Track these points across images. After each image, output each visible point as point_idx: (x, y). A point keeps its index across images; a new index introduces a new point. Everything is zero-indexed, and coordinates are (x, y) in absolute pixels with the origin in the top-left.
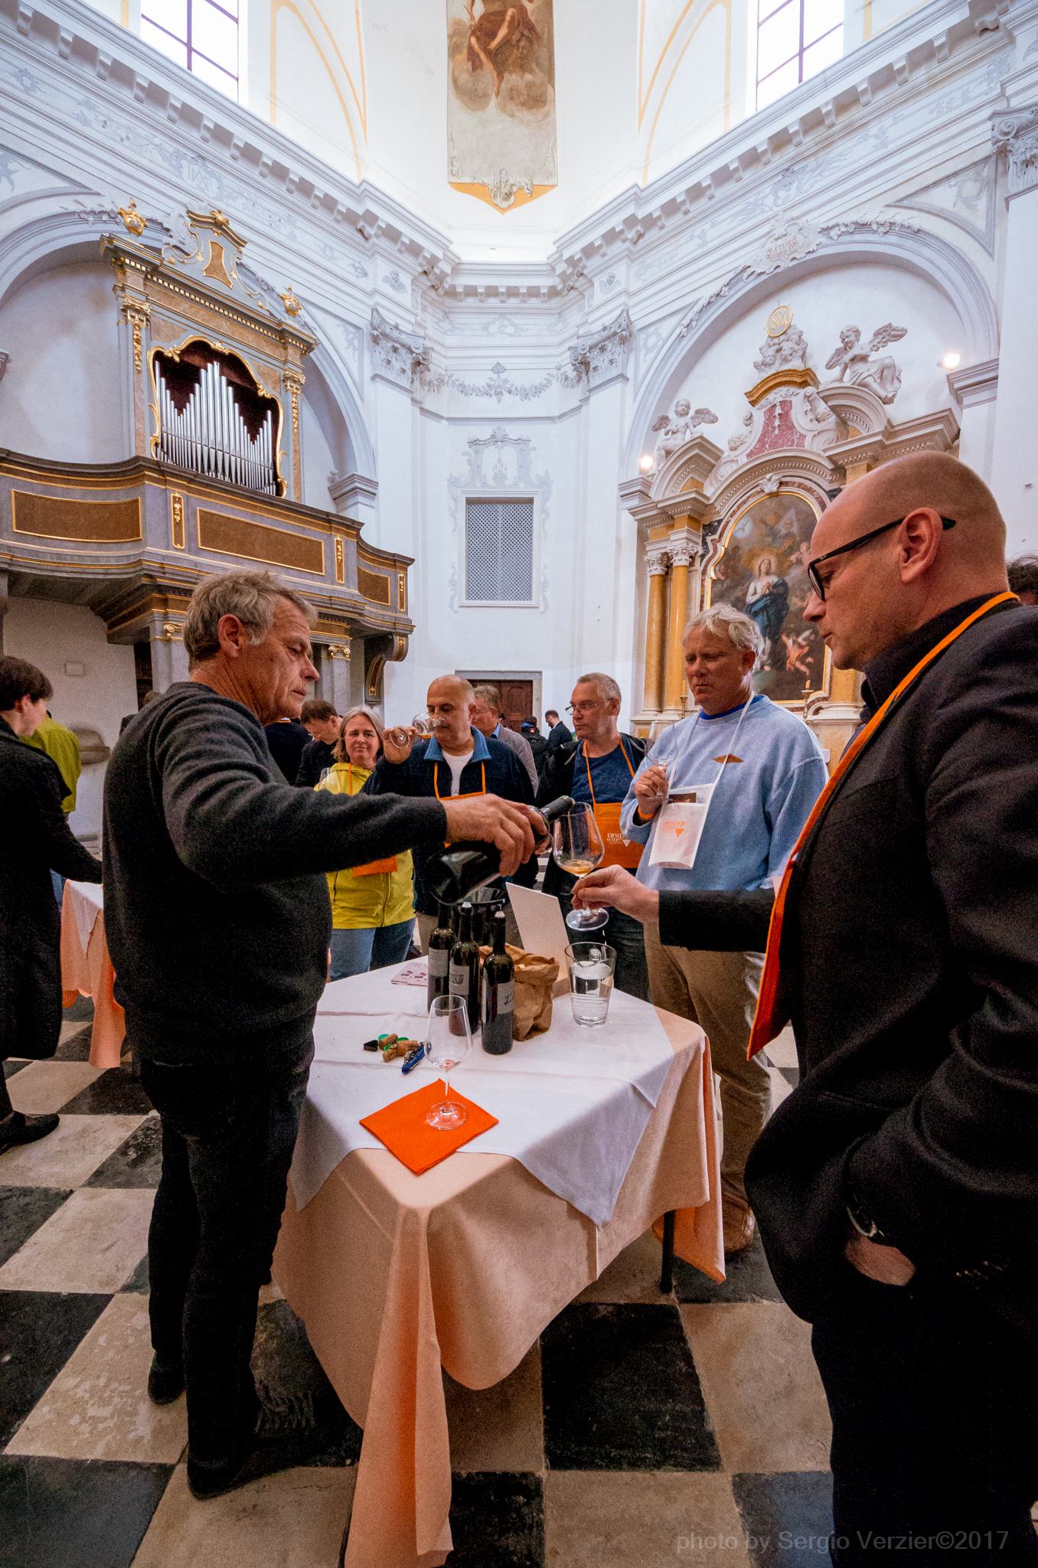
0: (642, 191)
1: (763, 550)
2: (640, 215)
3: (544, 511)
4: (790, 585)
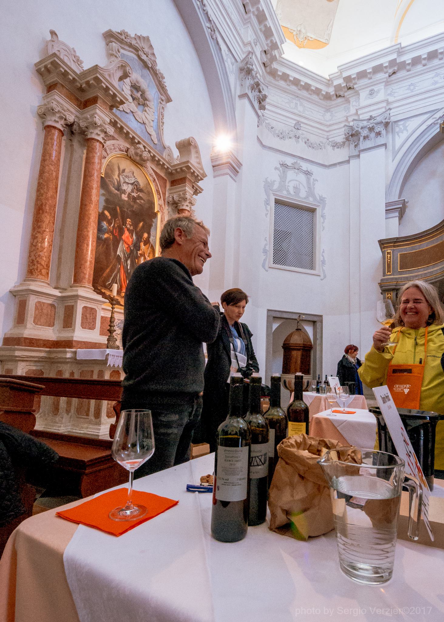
0: (402, 48)
2: (398, 61)
3: (323, 216)
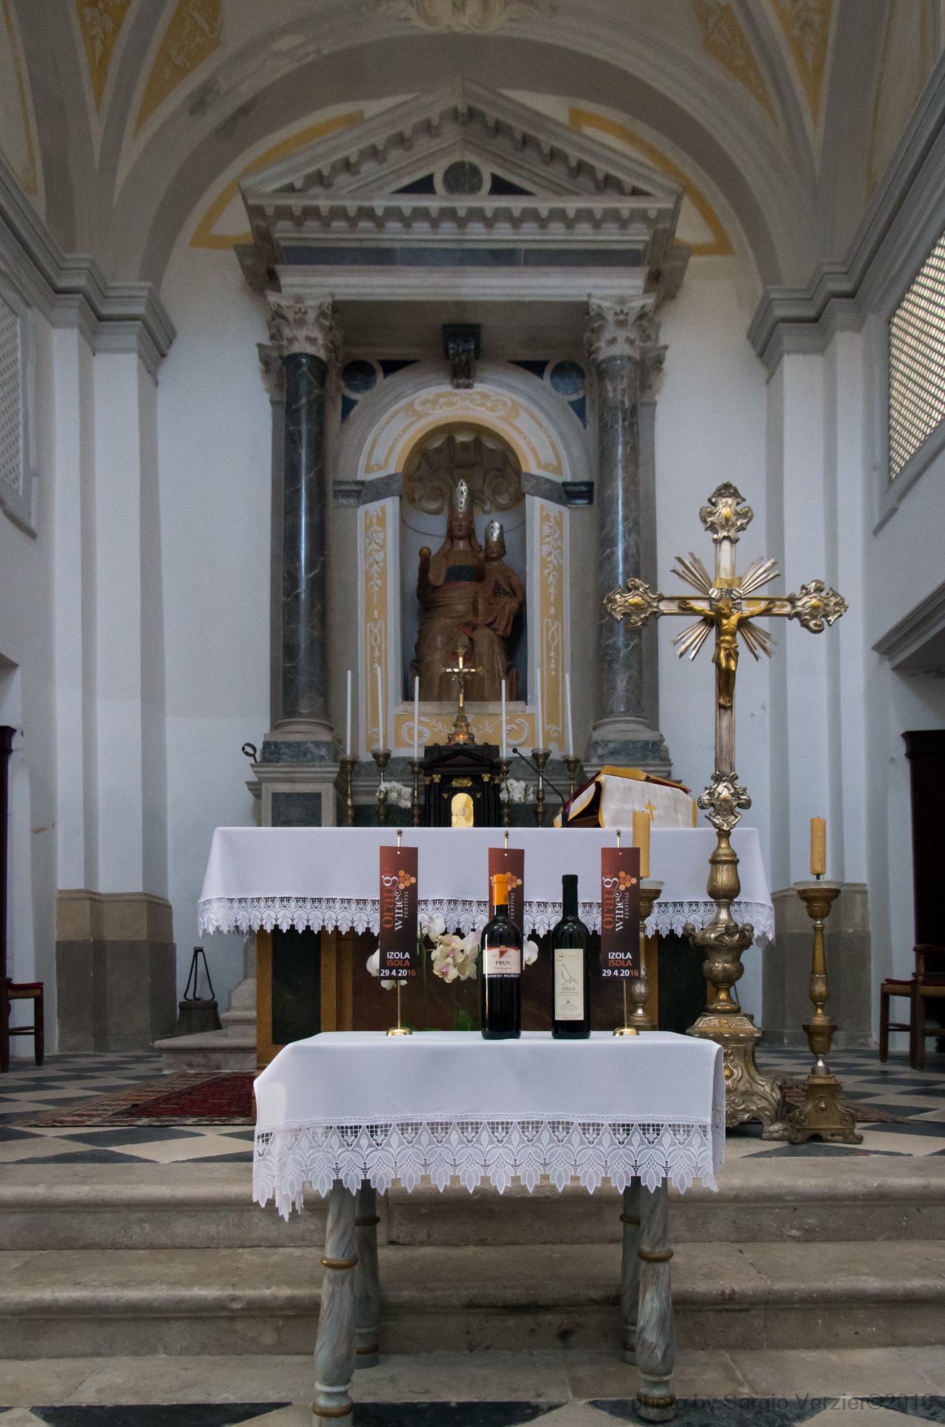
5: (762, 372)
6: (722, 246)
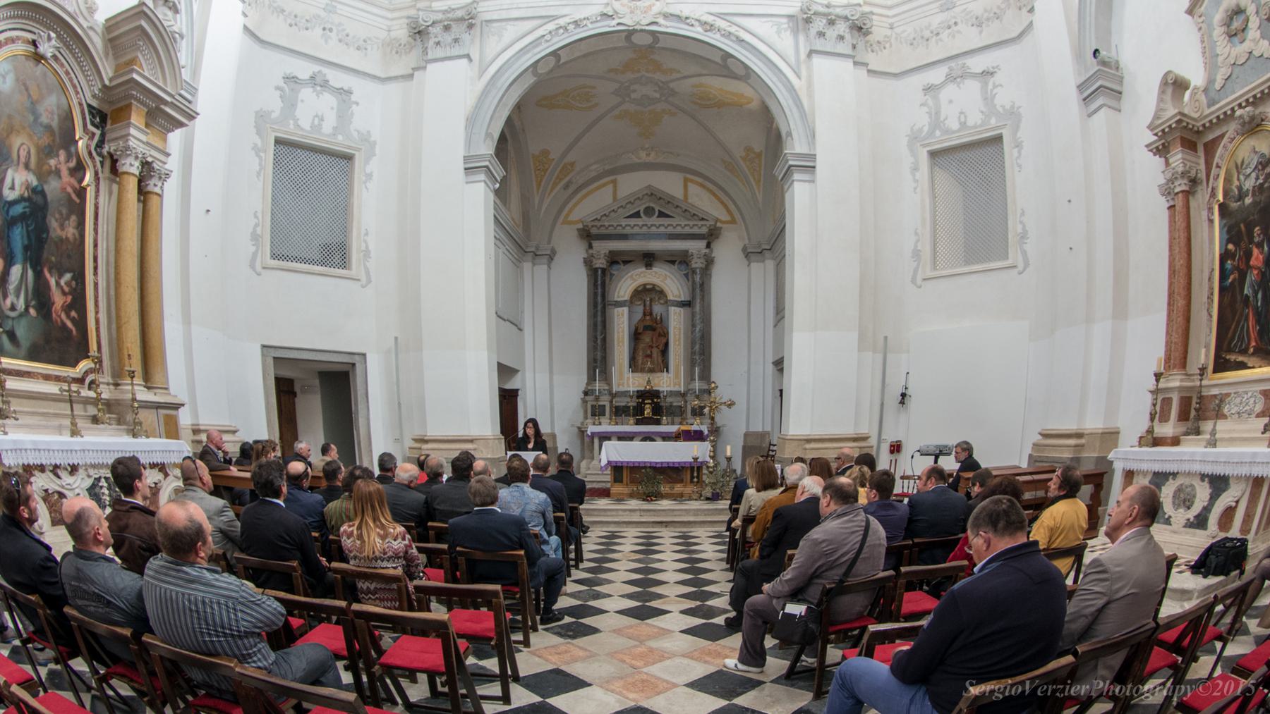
1: (24, 128)
4: (49, 198)
5: (747, 263)
6: (733, 221)
